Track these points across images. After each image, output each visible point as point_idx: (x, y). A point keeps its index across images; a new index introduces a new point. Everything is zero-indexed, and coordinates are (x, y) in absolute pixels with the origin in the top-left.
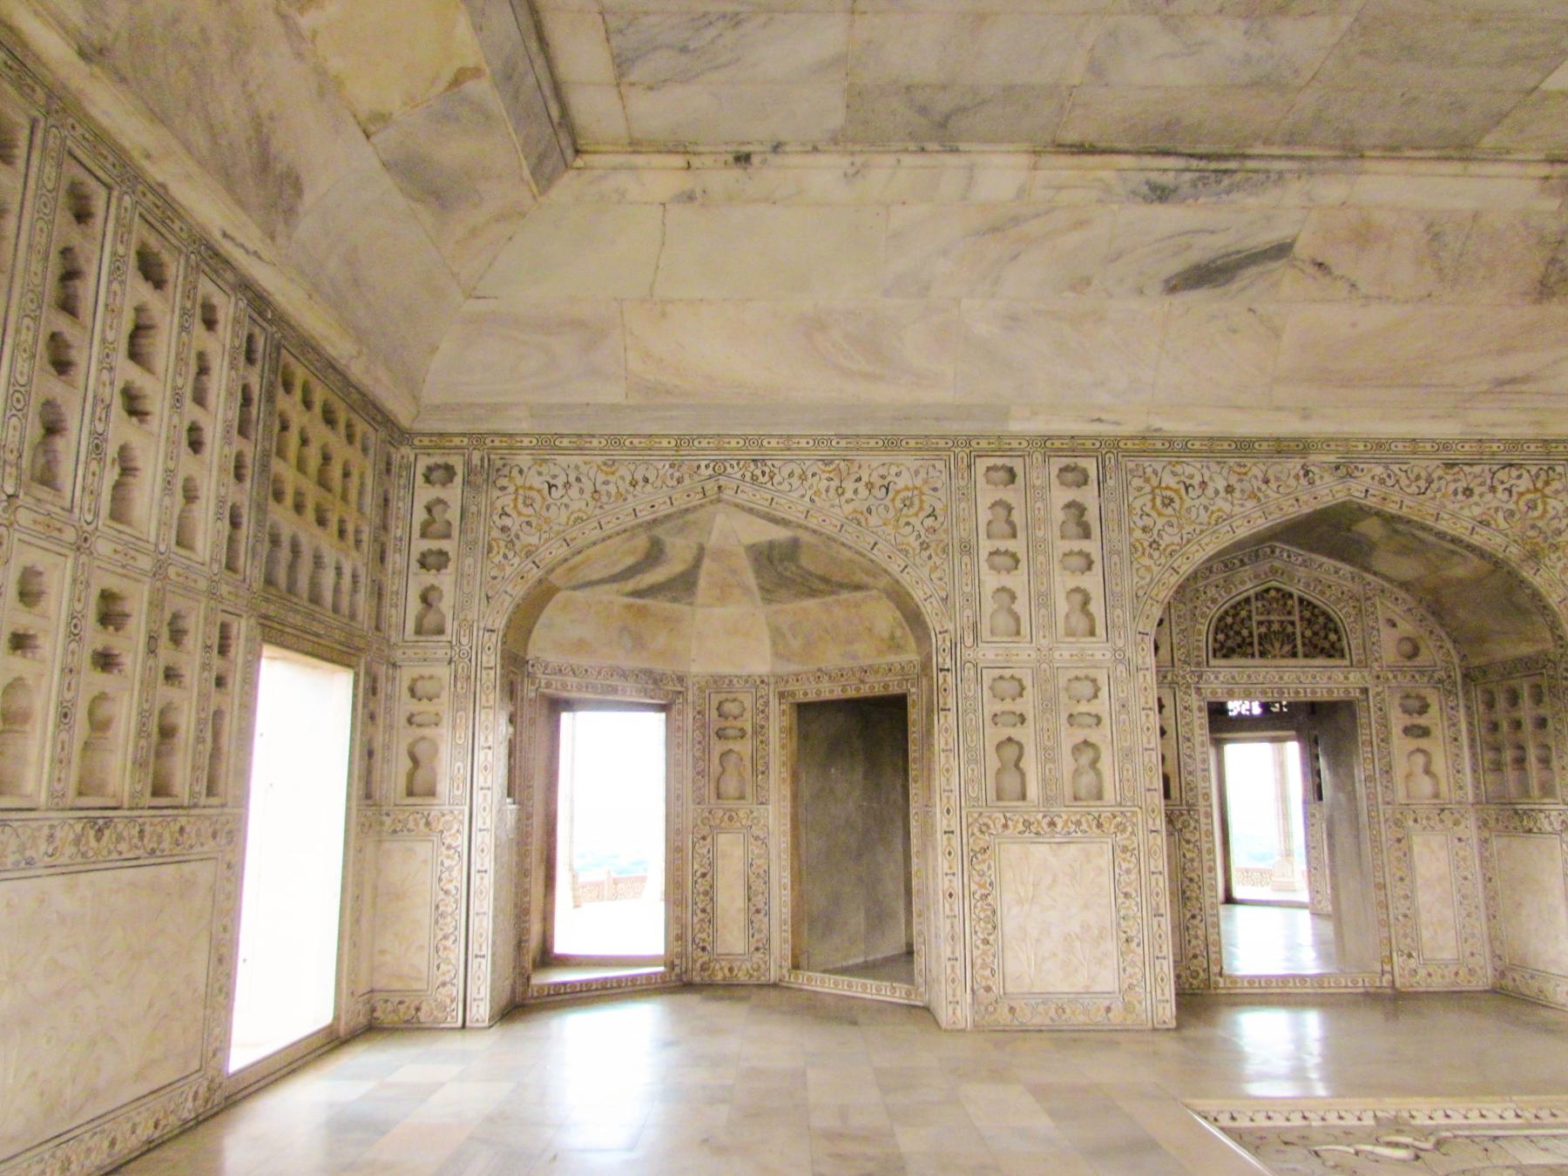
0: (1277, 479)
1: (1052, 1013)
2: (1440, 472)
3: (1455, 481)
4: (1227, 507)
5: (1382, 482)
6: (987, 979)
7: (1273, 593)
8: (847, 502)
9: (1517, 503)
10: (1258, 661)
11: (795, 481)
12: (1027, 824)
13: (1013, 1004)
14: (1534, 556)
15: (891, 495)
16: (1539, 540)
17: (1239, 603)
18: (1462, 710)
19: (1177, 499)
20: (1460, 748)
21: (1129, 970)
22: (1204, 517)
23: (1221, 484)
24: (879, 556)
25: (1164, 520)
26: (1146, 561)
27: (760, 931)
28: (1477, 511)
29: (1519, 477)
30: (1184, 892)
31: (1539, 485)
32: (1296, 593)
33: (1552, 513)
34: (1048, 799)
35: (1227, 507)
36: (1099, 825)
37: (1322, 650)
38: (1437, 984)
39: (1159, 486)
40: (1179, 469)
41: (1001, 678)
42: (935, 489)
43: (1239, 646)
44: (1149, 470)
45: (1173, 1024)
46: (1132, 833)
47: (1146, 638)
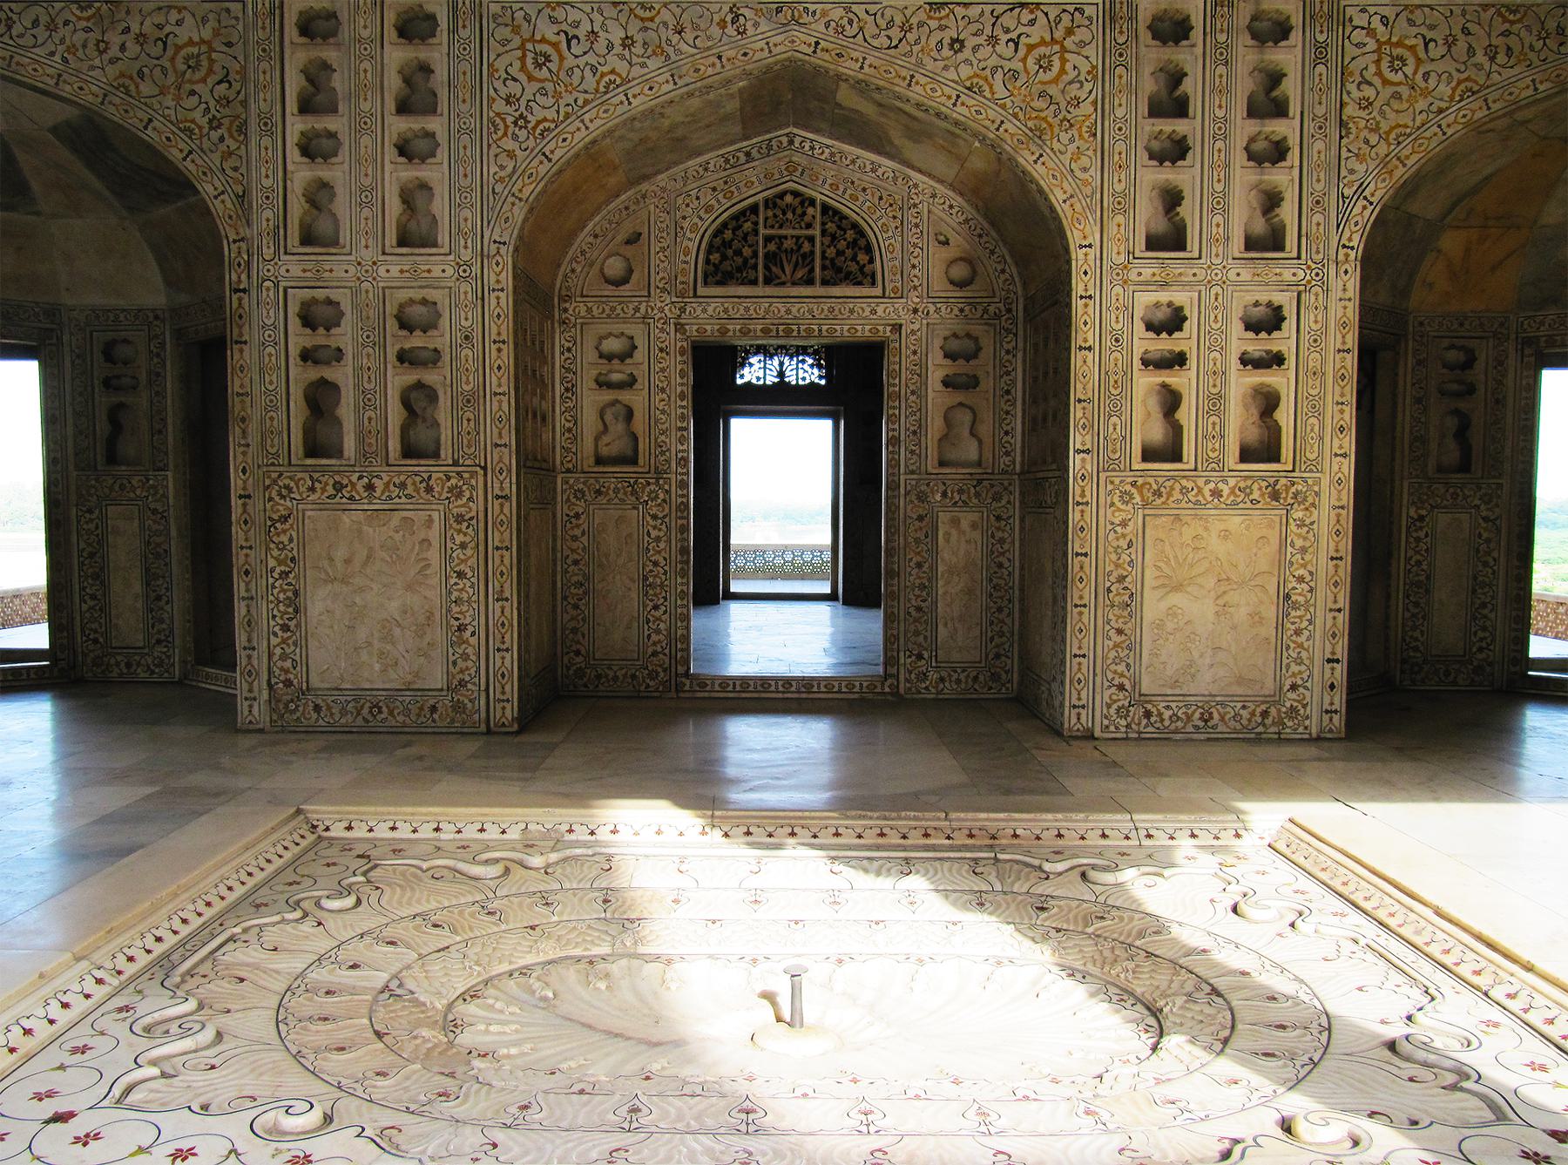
0: (696, 27)
1: (365, 711)
2: (922, 16)
3: (942, 28)
4: (622, 67)
5: (840, 30)
6: (287, 671)
7: (789, 198)
8: (112, 61)
9: (1024, 60)
10: (760, 290)
11: (42, 33)
12: (339, 487)
13: (319, 701)
14: (1038, 134)
15: (170, 52)
16: (1049, 114)
17: (743, 213)
18: (1020, 355)
19: (555, 57)
20: (1014, 404)
21: (461, 664)
22: (590, 82)
23: (617, 35)
24: (151, 135)
25: (536, 86)
26: (509, 144)
27: (162, 621)
28: (965, 71)
29: (1032, 22)
30: (645, 578)
31: (1058, 35)
32: (820, 197)
33: (1072, 74)
34: (364, 455)
35: (622, 67)
36: (429, 489)
37: (848, 274)
38: (949, 690)
39: (532, 39)
40: (559, 14)
41: (314, 301)
42: (229, 44)
43: (739, 270)
44: (519, 15)
45: (516, 727)
46: (470, 499)
47: (503, 249)
